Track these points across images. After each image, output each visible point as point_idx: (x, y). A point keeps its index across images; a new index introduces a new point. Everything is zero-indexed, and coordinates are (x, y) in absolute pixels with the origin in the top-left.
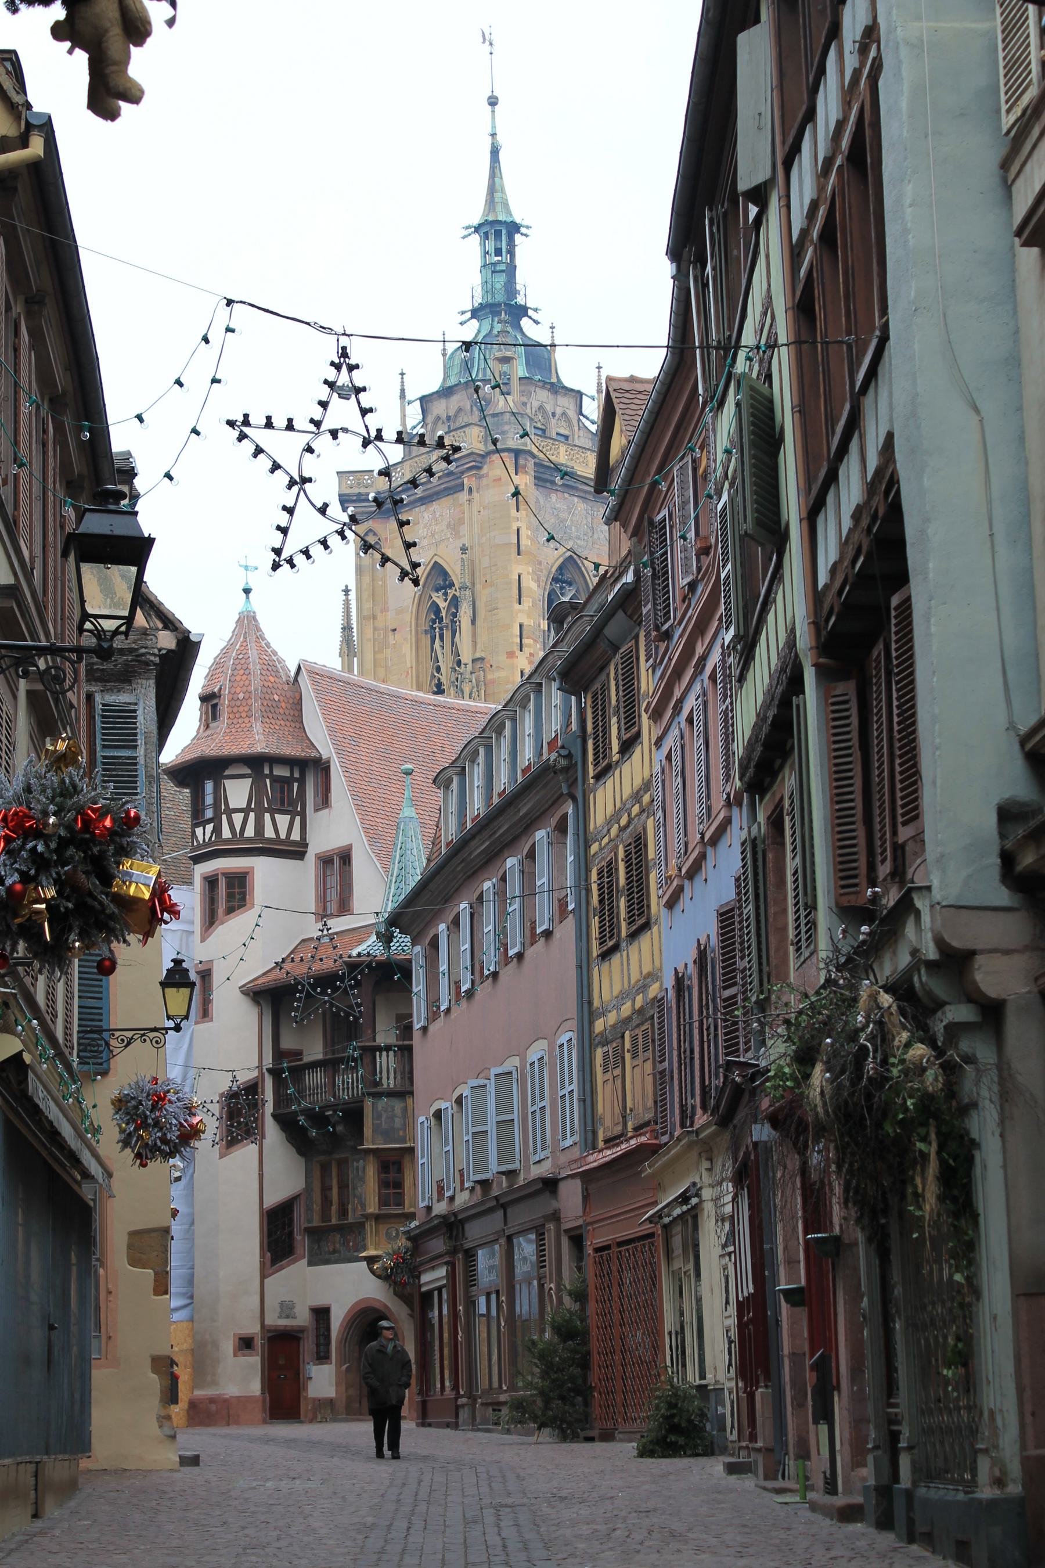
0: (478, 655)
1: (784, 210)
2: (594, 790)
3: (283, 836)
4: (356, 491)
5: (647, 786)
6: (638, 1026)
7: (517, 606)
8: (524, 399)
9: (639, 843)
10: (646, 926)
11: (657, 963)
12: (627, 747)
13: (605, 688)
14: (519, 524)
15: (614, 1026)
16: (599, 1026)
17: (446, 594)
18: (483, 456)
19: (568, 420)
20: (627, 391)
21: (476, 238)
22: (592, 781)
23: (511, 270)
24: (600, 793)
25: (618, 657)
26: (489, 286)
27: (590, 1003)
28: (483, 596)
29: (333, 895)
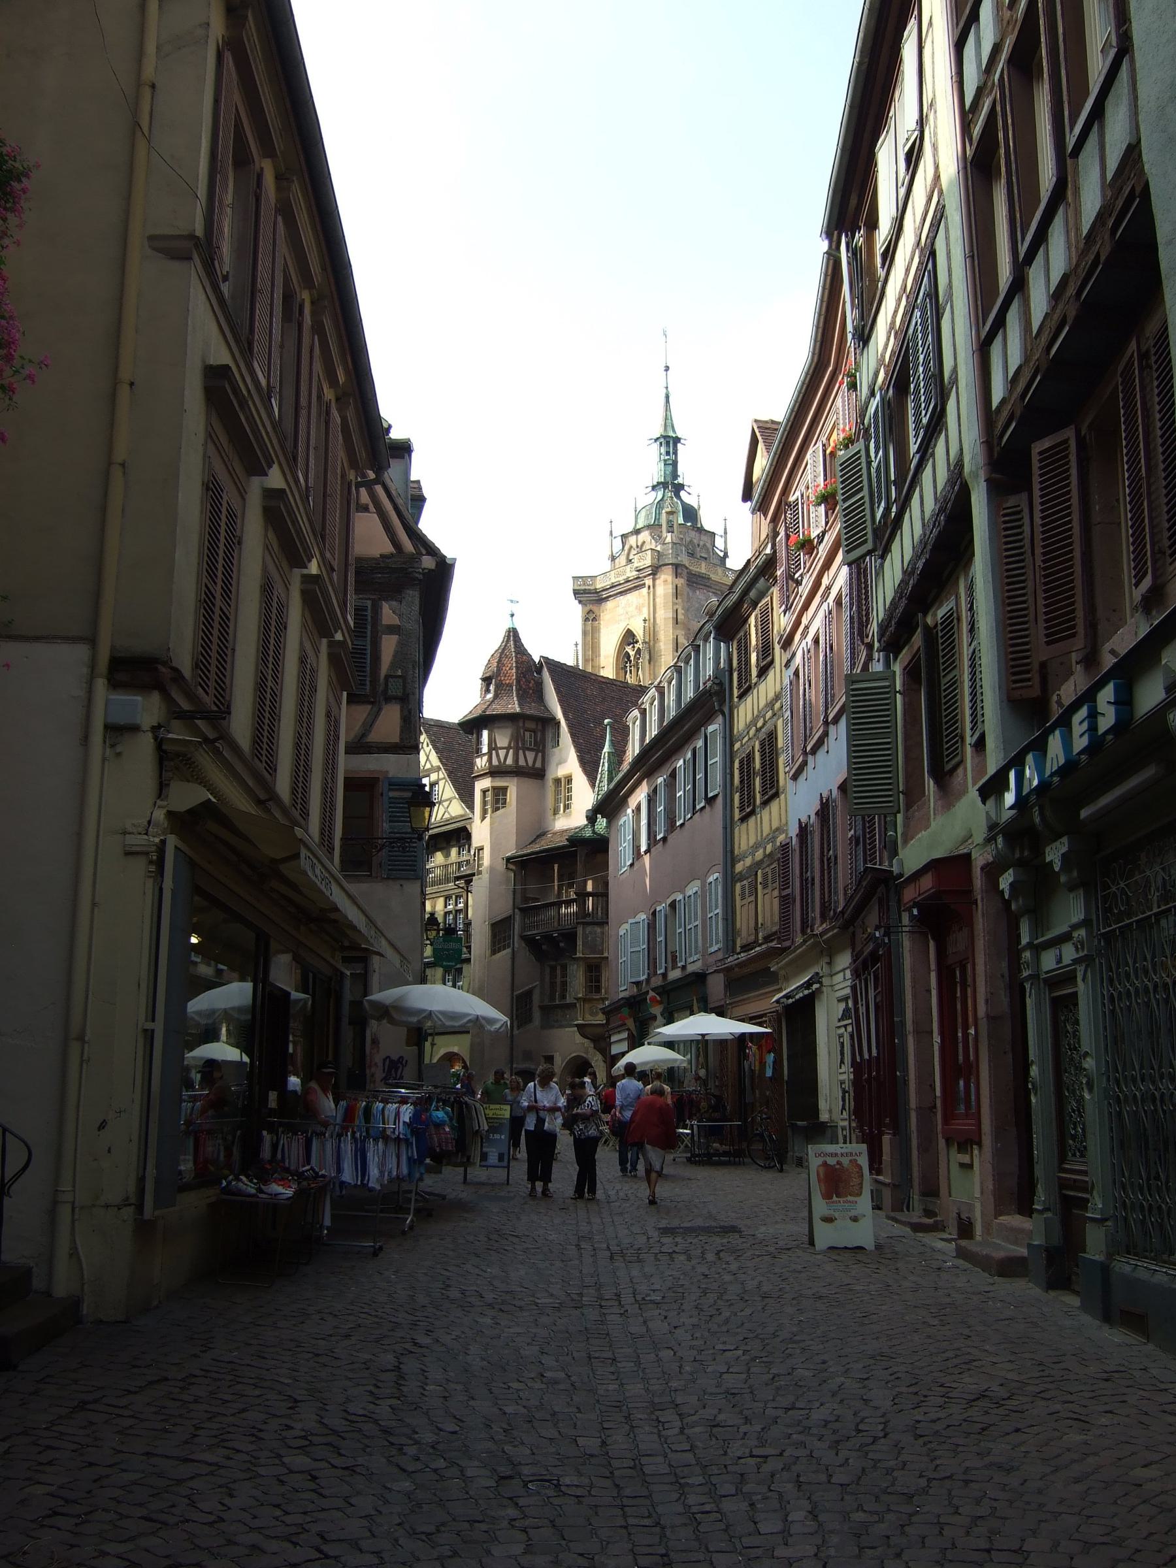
2: (738, 707)
4: (583, 588)
5: (777, 697)
6: (769, 866)
9: (772, 736)
10: (776, 795)
11: (784, 821)
12: (763, 671)
13: (747, 635)
15: (750, 868)
16: (739, 867)
19: (708, 549)
21: (656, 445)
22: (736, 700)
23: (675, 464)
24: (742, 708)
25: (757, 611)
27: (732, 851)
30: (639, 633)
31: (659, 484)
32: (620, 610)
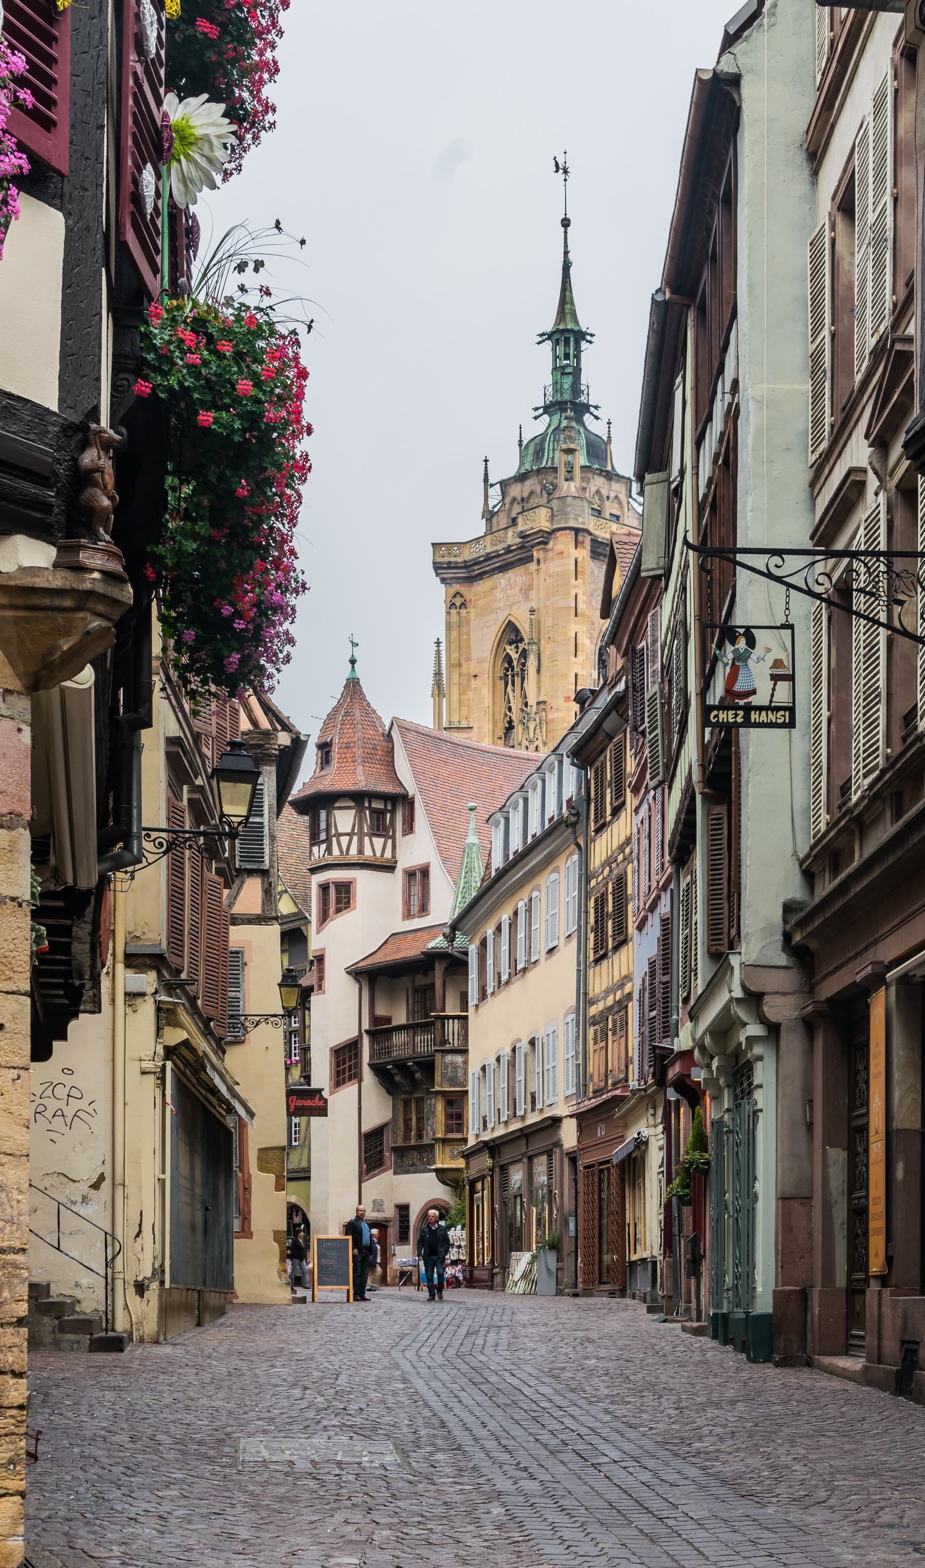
0: (541, 699)
1: (695, 476)
3: (378, 854)
4: (447, 559)
7: (573, 658)
8: (584, 485)
14: (576, 591)
17: (517, 647)
18: (550, 533)
19: (620, 503)
20: (626, 543)
21: (548, 345)
23: (577, 372)
26: (559, 386)
28: (547, 649)
29: (415, 902)
30: (525, 634)
31: (552, 404)
32: (499, 594)
